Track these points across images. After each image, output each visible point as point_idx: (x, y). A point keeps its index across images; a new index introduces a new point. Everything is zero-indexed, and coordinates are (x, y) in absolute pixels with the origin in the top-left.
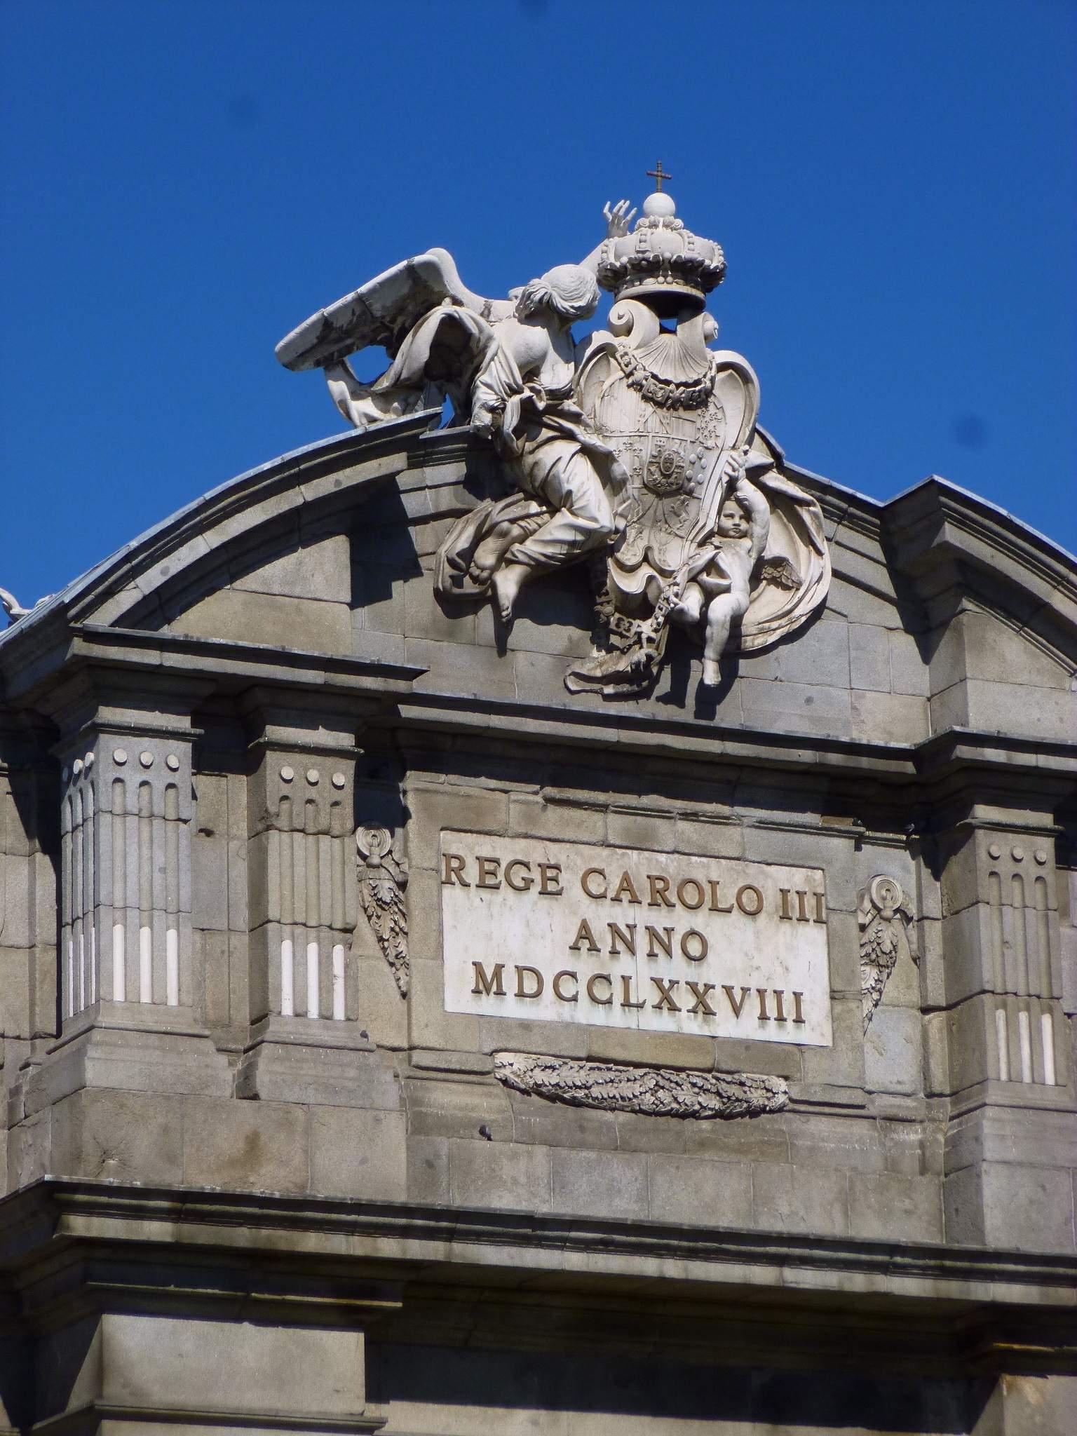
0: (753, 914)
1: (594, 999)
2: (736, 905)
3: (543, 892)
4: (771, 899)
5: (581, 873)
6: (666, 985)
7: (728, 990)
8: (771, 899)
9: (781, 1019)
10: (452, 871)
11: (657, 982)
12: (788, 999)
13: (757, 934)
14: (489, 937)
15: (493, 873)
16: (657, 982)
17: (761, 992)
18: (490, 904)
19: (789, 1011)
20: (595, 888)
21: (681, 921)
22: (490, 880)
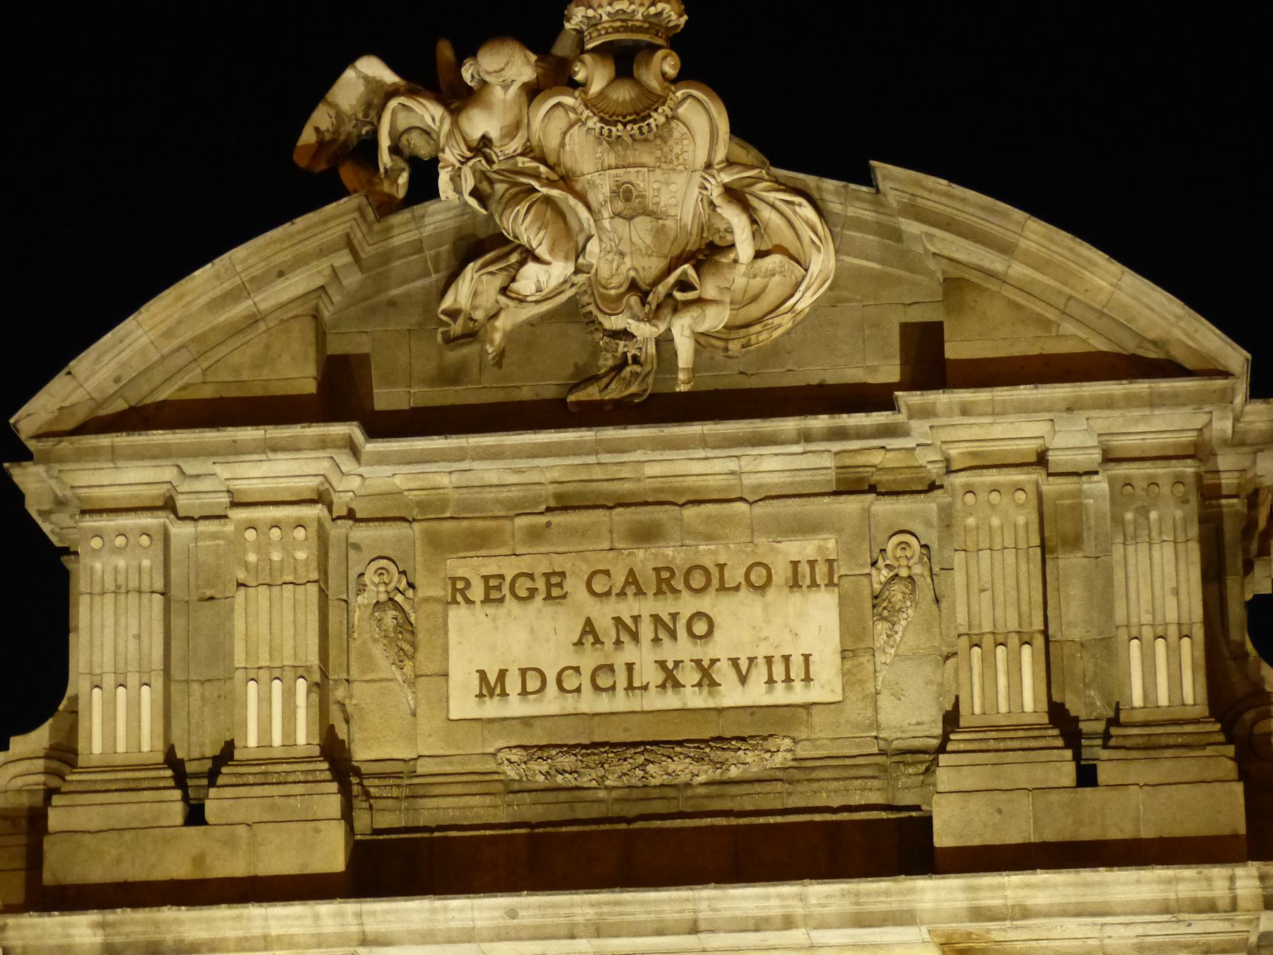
0: (762, 589)
1: (597, 688)
2: (743, 583)
3: (549, 597)
4: (781, 572)
5: (586, 577)
6: (670, 665)
7: (735, 662)
8: (781, 572)
9: (788, 680)
10: (458, 591)
11: (662, 664)
12: (797, 662)
13: (766, 608)
14: (493, 647)
15: (499, 588)
16: (662, 664)
17: (769, 660)
18: (494, 619)
19: (797, 670)
20: (598, 588)
21: (687, 605)
22: (494, 595)
